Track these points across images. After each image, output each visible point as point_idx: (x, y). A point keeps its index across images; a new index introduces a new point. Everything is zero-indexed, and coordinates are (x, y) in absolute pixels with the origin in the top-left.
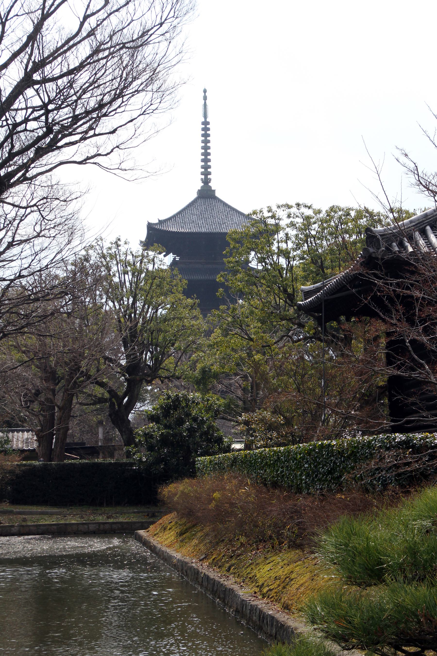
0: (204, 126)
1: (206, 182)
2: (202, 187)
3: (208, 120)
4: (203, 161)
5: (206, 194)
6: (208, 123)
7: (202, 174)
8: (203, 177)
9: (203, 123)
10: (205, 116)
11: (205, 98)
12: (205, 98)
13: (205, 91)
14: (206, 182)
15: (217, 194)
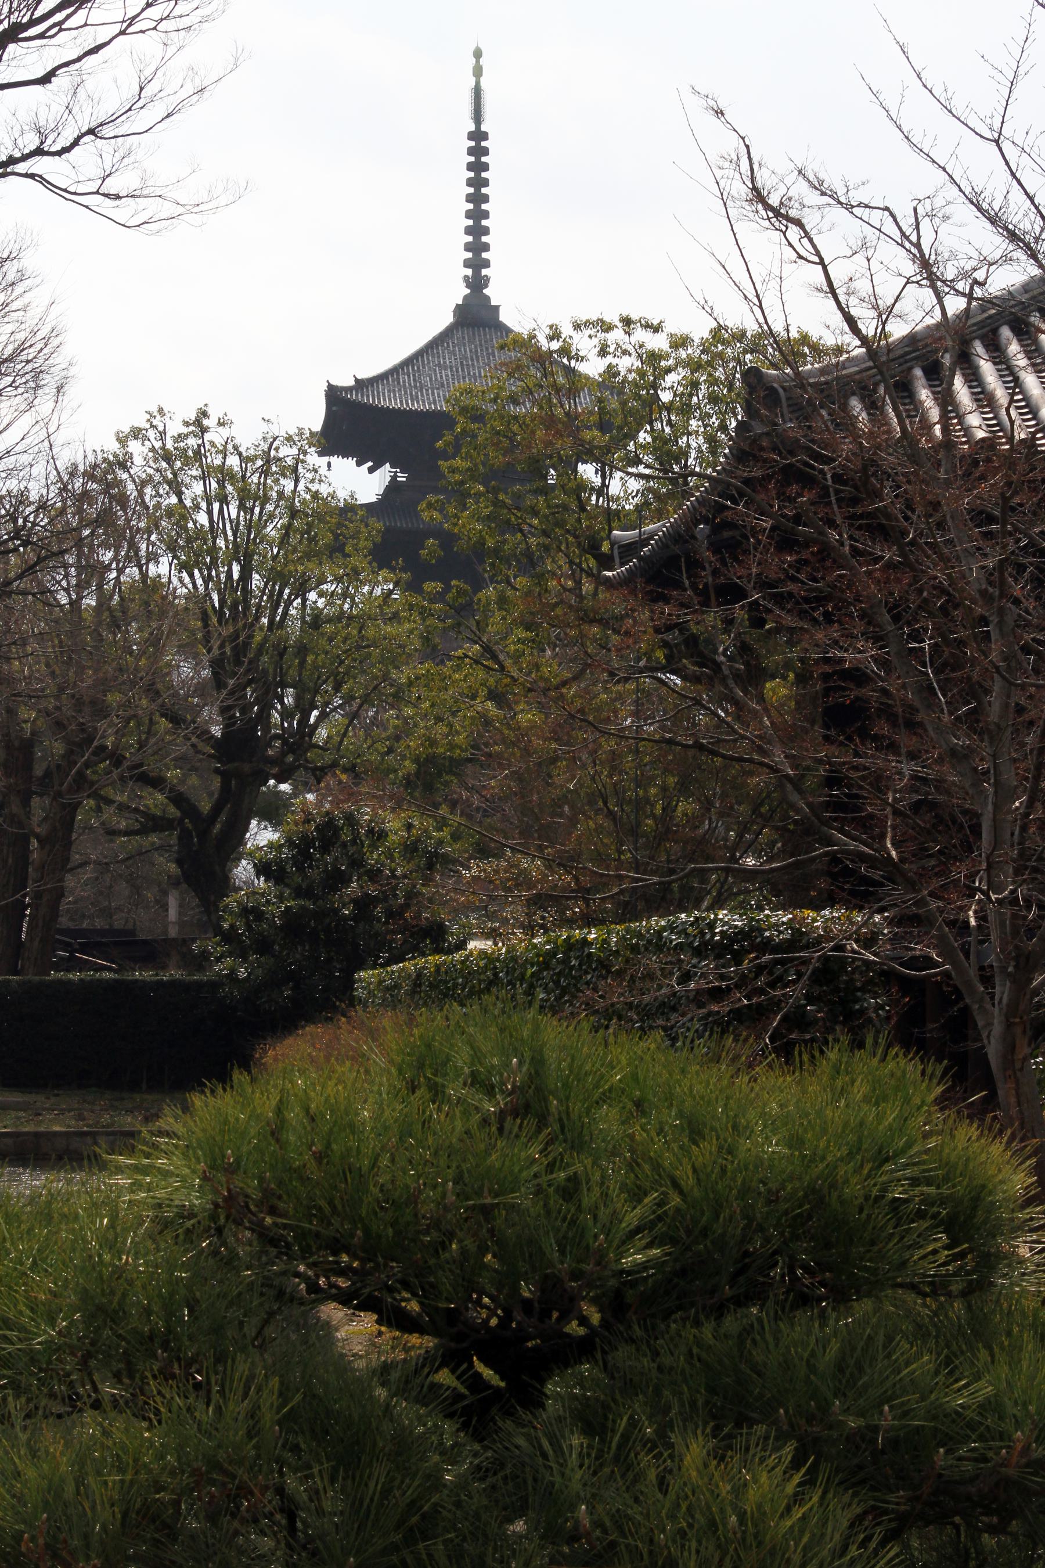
0: (473, 143)
1: (477, 283)
2: (465, 298)
3: (483, 128)
4: (468, 231)
5: (476, 316)
6: (485, 136)
7: (467, 264)
8: (469, 272)
9: (471, 136)
10: (478, 116)
11: (478, 72)
12: (478, 72)
13: (478, 54)
14: (477, 283)
15: (505, 317)
